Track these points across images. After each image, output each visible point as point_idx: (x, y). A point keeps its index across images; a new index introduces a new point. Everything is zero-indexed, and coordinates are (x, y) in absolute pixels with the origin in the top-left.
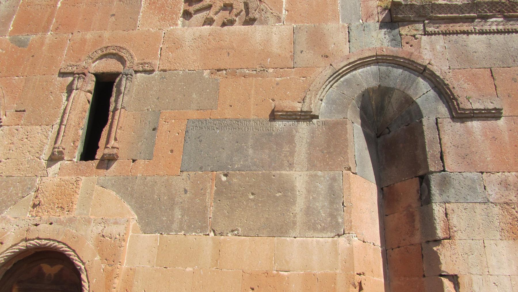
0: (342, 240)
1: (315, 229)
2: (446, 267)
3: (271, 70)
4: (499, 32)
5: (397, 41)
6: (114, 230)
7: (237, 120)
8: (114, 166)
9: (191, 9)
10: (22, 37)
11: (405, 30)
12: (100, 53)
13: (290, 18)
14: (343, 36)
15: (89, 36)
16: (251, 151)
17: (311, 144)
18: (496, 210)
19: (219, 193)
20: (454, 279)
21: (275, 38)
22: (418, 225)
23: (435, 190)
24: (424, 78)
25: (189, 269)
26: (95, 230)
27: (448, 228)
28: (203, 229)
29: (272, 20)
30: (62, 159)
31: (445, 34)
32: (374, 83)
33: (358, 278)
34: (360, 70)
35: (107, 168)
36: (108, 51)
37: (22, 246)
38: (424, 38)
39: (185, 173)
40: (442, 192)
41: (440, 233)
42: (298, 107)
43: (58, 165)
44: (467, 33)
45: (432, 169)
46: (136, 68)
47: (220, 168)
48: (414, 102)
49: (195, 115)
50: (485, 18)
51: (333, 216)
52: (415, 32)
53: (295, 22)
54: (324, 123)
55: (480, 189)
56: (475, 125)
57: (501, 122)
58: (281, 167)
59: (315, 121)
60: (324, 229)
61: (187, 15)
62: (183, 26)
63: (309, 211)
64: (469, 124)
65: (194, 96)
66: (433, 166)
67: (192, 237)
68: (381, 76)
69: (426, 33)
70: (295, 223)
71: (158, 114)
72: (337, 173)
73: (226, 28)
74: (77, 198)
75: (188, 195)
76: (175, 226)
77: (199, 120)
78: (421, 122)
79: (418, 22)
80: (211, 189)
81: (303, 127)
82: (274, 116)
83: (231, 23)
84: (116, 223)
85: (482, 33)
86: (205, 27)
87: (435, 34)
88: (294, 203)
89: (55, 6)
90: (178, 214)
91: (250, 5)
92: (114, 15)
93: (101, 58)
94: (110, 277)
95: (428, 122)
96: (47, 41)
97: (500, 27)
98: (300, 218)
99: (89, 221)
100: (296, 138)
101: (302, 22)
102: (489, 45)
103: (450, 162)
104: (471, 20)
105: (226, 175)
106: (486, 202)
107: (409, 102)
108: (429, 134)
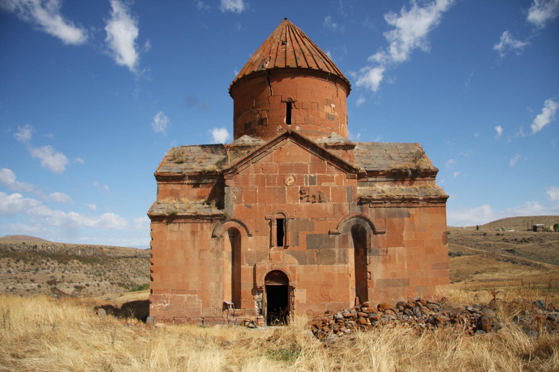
0: (347, 265)
1: (340, 263)
2: (369, 270)
3: (328, 219)
4: (389, 207)
5: (362, 210)
6: (293, 265)
7: (320, 235)
8: (289, 248)
9: (302, 196)
10: (248, 204)
11: (364, 206)
12: (277, 212)
13: (333, 201)
14: (347, 208)
15: (271, 205)
16: (324, 243)
17: (339, 241)
18: (381, 257)
19: (317, 255)
20: (370, 273)
21: (329, 207)
22: (363, 260)
23: (368, 253)
24: (368, 222)
25: (312, 273)
26: (289, 265)
27: (370, 261)
28: (314, 264)
29: (327, 201)
30: (274, 246)
31: (375, 207)
32: (355, 223)
33: (350, 273)
34: (352, 219)
35: (287, 248)
36: (279, 212)
37: (271, 270)
38: (369, 209)
39: (308, 250)
40: (369, 253)
41: (368, 263)
42: (336, 231)
43: (273, 248)
44: (381, 207)
45: (368, 247)
46: (289, 218)
47: (317, 248)
48: (365, 229)
49: (308, 233)
50: (385, 203)
51: (344, 260)
52: (367, 206)
53: (334, 202)
54: (343, 235)
55: (378, 252)
56: (379, 235)
57: (385, 235)
58: (332, 248)
59: (340, 235)
60: (342, 263)
61: (301, 198)
62: (301, 202)
63: (339, 259)
64: (378, 235)
65: (307, 227)
66: (368, 247)
67: (312, 265)
68: (357, 221)
69: (370, 207)
70: (336, 262)
71: (298, 233)
72: (346, 249)
73: (314, 204)
74: (281, 257)
75: (310, 255)
76: (307, 263)
77: (309, 235)
78: (366, 235)
79: (367, 203)
80: (315, 254)
81: (337, 236)
82: (329, 233)
83: (315, 202)
84: (294, 264)
85: (384, 207)
86: (308, 203)
87: (372, 207)
88: (335, 257)
89: (256, 192)
90: (308, 260)
91: (321, 196)
92: (277, 197)
93: (277, 214)
94: (294, 276)
95: (368, 235)
96: (258, 206)
97: (389, 206)
98: (337, 260)
99: (286, 264)
100: (336, 240)
101: (336, 202)
102: (386, 211)
103: (372, 246)
104: (382, 203)
105: (318, 250)
106: (379, 255)
107: (363, 228)
108: (368, 238)
